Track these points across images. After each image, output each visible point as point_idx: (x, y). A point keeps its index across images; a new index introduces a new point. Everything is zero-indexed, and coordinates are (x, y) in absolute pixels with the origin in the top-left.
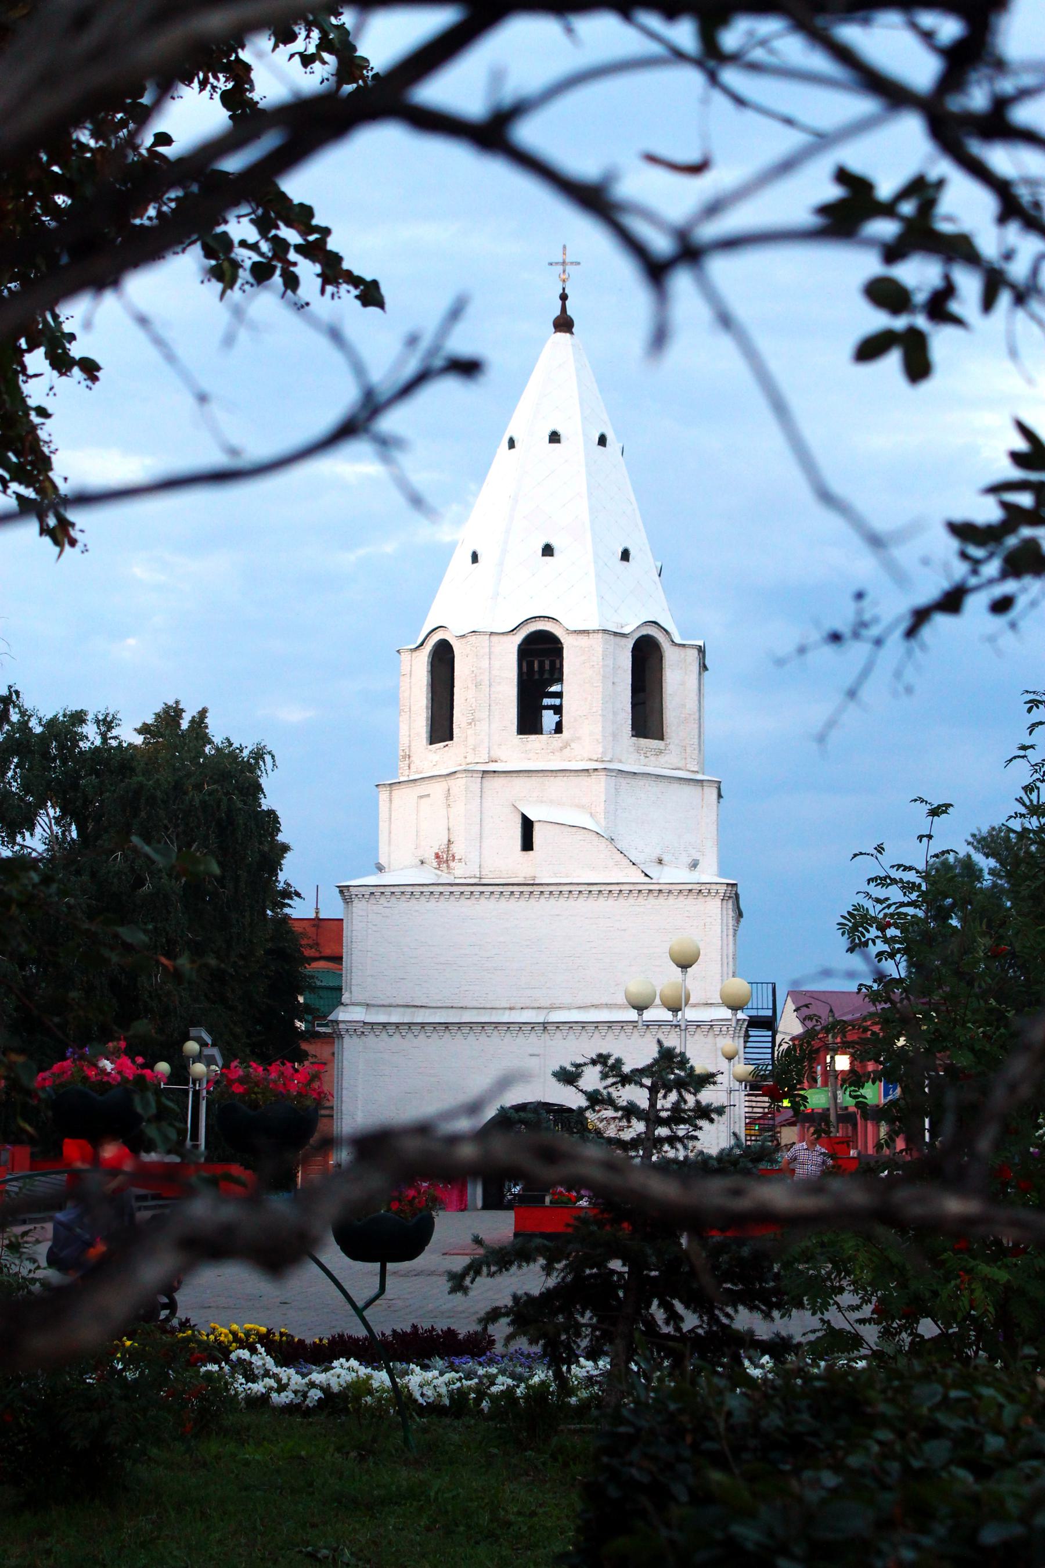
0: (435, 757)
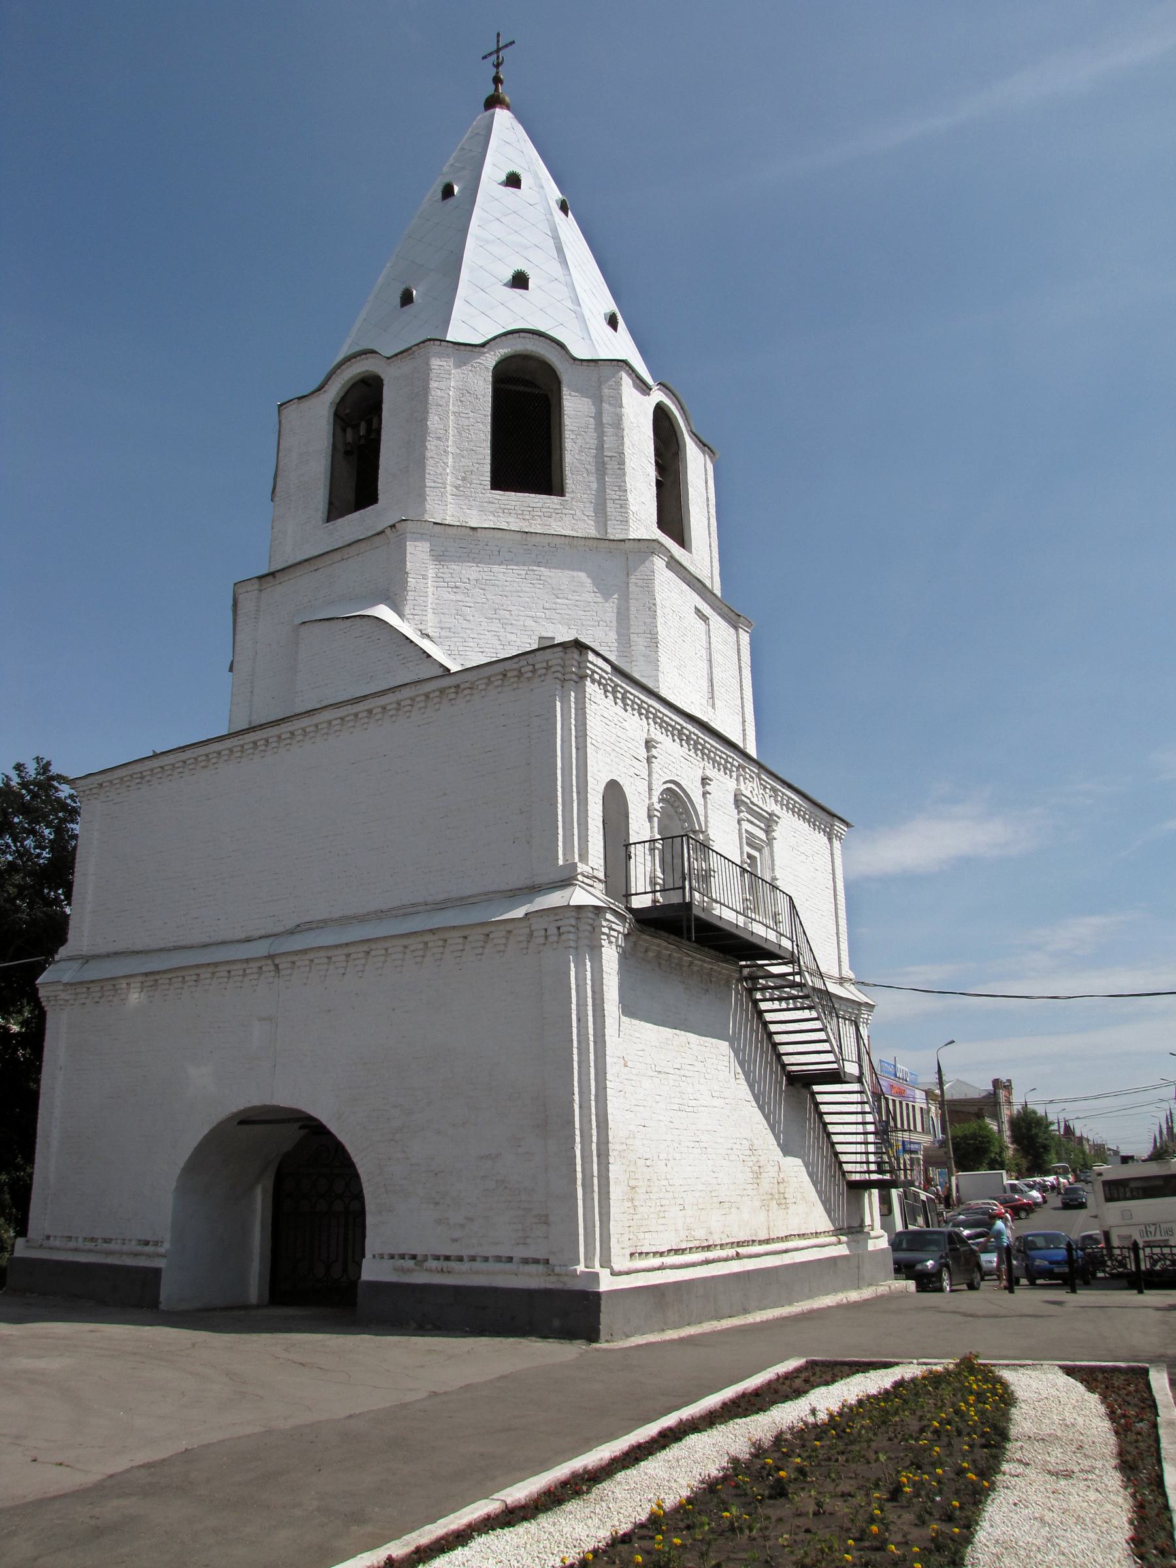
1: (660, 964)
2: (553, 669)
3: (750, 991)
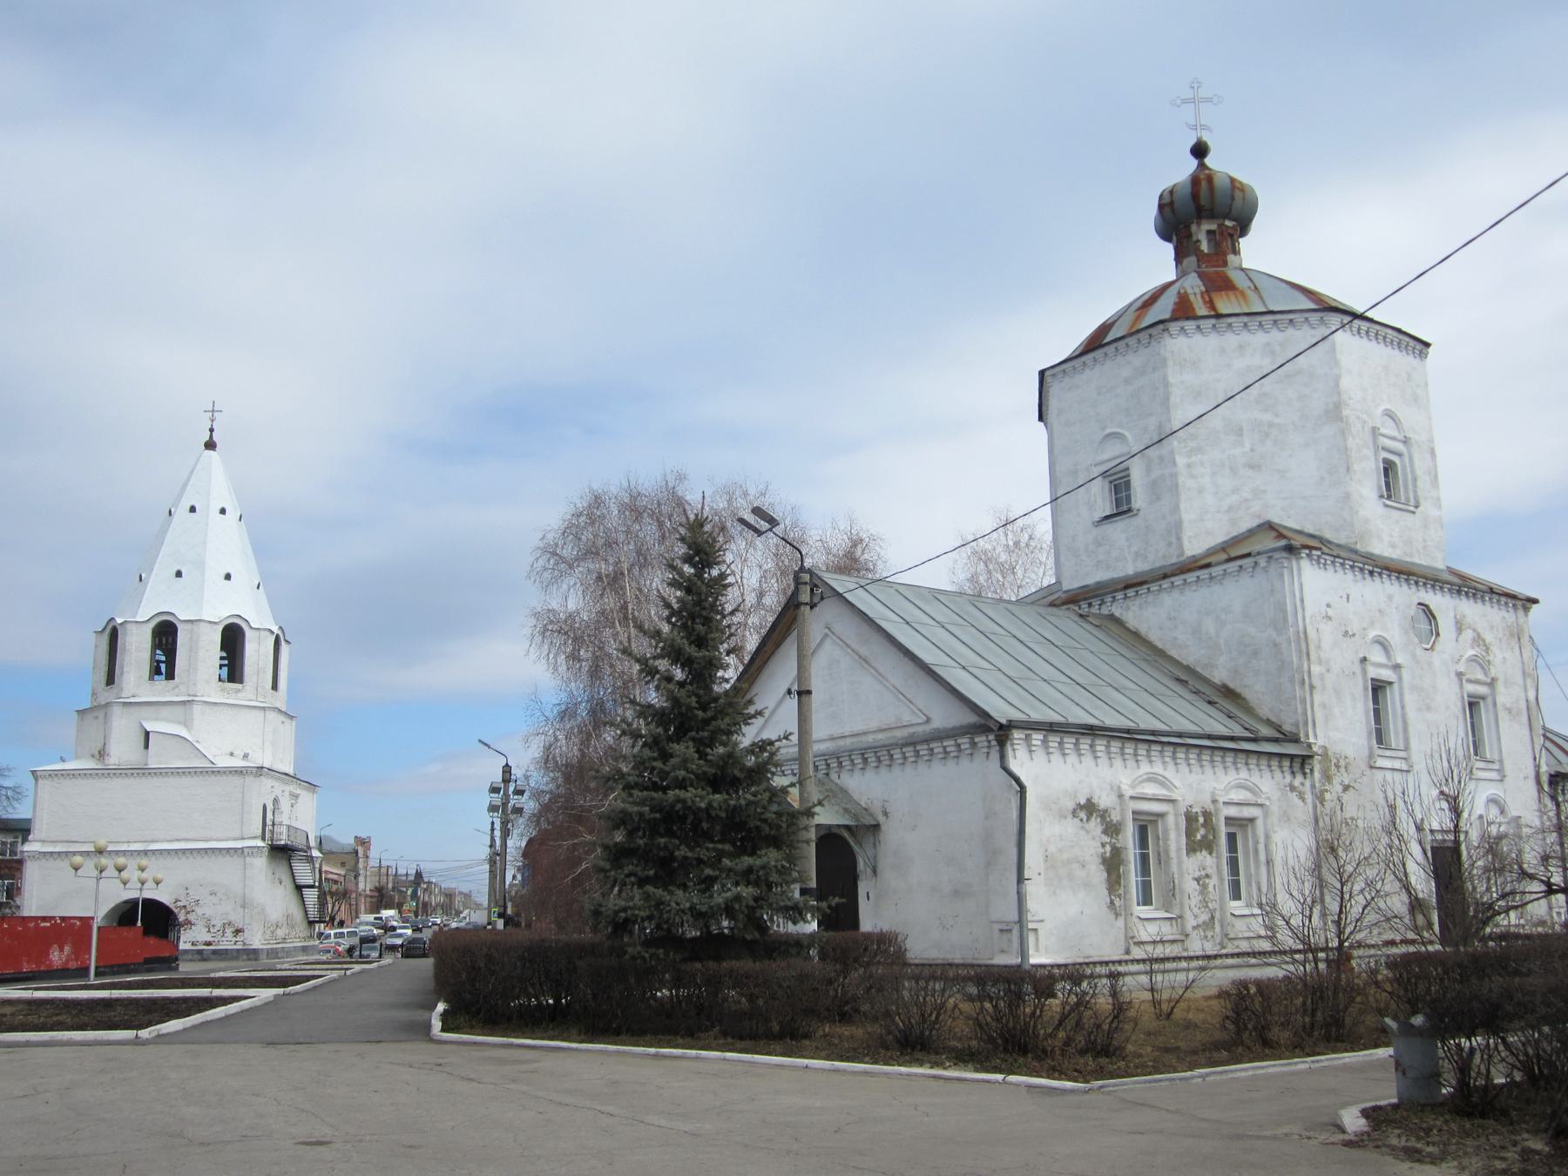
0: (106, 694)
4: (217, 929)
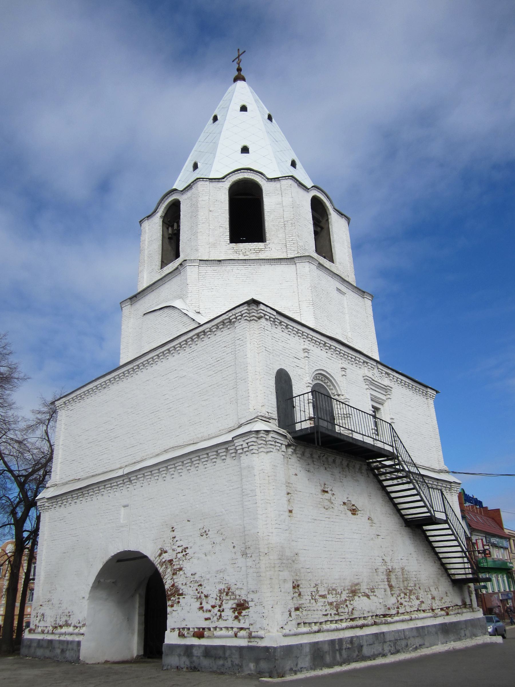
1: (313, 461)
2: (244, 315)
3: (376, 476)
4: (212, 602)
